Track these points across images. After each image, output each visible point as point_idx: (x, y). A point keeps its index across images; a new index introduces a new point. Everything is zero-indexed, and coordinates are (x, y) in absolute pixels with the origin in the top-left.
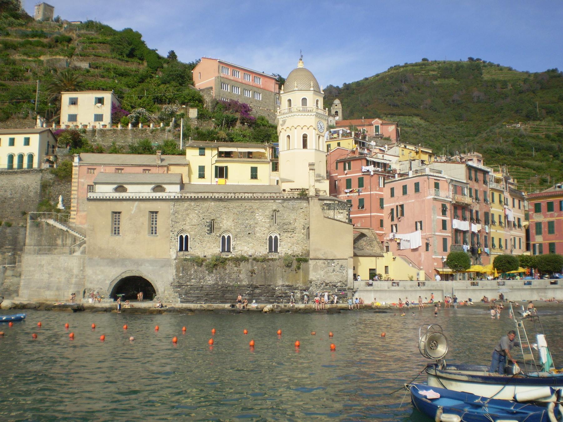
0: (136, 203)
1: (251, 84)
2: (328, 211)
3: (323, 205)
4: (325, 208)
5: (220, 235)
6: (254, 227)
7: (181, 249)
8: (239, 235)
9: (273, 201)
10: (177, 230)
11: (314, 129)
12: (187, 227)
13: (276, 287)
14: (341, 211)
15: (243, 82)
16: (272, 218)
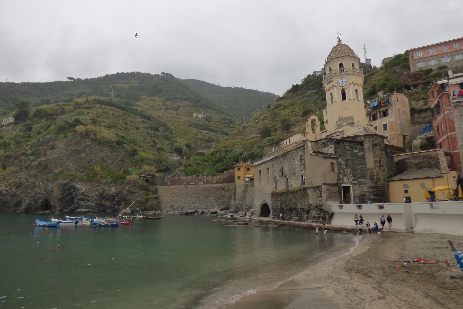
0: (264, 165)
1: (450, 51)
2: (324, 149)
3: (322, 144)
4: (323, 146)
5: (285, 177)
6: (295, 169)
7: (277, 188)
8: (291, 176)
9: (299, 150)
10: (274, 176)
11: (335, 86)
12: (276, 175)
13: (299, 209)
14: (331, 146)
15: (440, 53)
16: (300, 161)
